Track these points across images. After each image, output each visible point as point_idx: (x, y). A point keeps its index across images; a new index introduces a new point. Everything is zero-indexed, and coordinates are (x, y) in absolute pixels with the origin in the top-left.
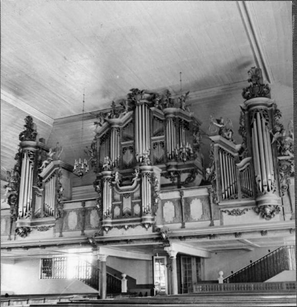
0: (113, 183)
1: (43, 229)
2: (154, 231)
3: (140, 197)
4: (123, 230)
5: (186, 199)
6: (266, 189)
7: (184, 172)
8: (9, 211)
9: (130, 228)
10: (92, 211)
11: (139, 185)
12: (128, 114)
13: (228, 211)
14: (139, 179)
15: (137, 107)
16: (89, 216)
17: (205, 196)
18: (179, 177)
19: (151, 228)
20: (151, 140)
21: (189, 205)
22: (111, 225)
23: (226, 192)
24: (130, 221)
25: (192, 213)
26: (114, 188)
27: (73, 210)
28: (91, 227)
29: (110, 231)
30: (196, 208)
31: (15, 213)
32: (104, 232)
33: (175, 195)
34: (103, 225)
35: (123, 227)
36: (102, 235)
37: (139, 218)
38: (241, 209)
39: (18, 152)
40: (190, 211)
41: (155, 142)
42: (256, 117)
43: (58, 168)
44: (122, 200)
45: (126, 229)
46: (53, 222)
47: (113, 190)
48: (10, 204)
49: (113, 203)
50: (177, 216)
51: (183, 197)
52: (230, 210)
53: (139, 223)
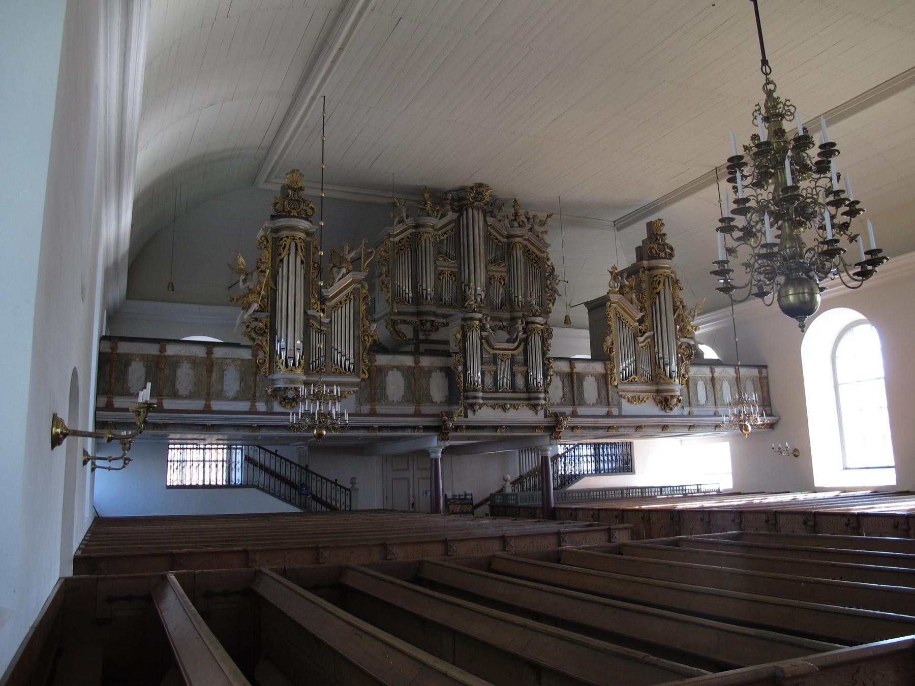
0: (484, 334)
2: (545, 417)
3: (526, 363)
5: (578, 374)
9: (512, 410)
10: (434, 374)
11: (523, 344)
12: (451, 216)
14: (525, 336)
15: (470, 211)
16: (428, 384)
19: (541, 413)
20: (487, 271)
22: (481, 401)
25: (586, 395)
27: (395, 367)
28: (433, 402)
32: (469, 412)
34: (470, 401)
36: (466, 416)
37: (524, 396)
40: (582, 393)
43: (359, 286)
44: (495, 363)
45: (504, 408)
46: (357, 385)
47: (481, 344)
48: (253, 339)
49: (483, 367)
50: (567, 397)
51: (575, 370)
52: (629, 395)
53: (526, 402)
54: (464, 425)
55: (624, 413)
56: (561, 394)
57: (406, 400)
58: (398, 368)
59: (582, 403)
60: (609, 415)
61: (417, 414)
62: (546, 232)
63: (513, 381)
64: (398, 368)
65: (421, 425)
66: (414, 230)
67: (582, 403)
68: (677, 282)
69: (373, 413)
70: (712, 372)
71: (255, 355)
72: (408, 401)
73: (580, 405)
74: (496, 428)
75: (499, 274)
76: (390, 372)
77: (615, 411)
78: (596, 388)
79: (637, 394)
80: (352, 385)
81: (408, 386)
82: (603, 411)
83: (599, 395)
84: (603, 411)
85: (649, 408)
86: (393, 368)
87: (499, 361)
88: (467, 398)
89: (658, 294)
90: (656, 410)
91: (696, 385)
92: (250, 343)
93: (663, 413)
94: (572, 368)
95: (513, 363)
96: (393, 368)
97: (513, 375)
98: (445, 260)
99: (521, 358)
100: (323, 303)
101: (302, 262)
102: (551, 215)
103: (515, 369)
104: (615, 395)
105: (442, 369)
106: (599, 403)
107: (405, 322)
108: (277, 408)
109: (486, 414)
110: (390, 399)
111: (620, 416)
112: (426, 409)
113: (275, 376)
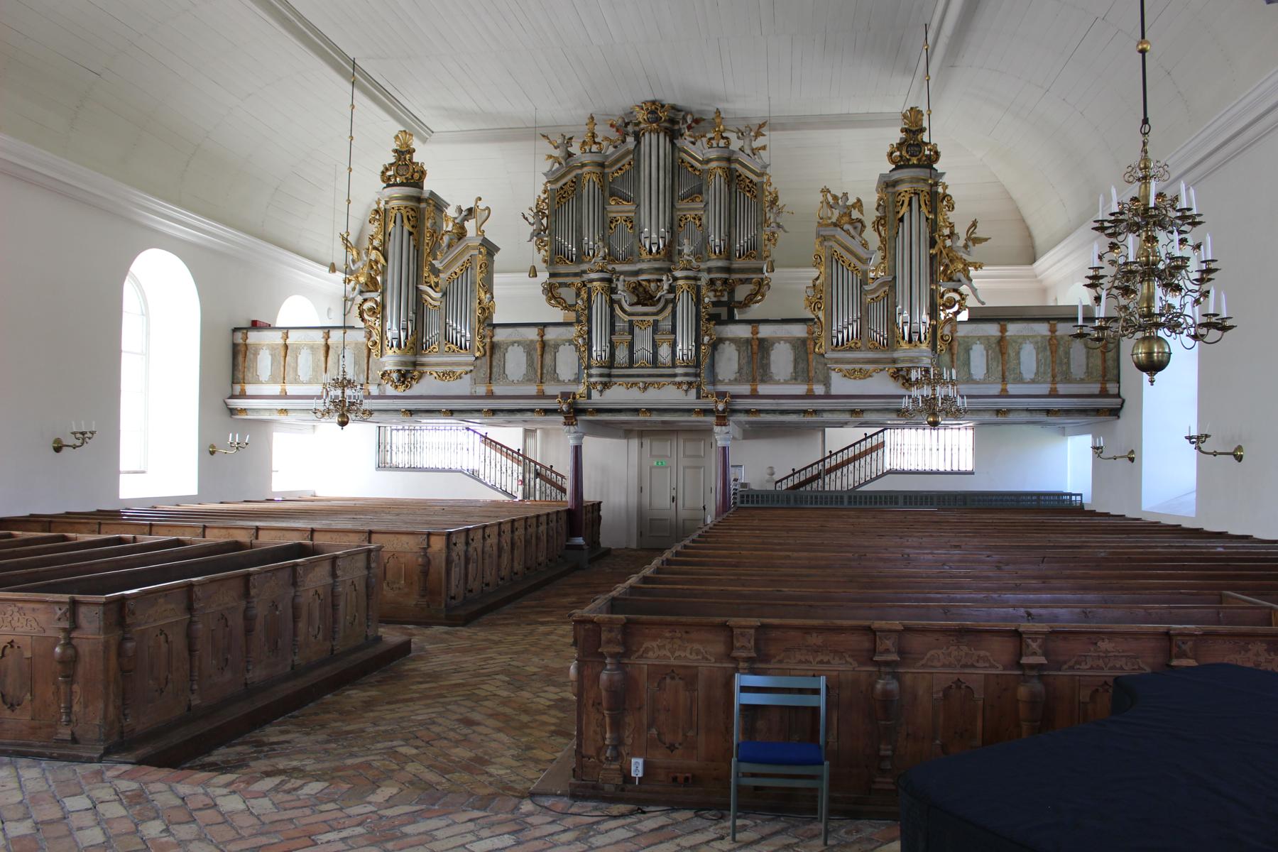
0: (614, 296)
1: (445, 375)
2: (698, 397)
4: (635, 389)
5: (762, 341)
6: (915, 337)
7: (743, 282)
8: (362, 333)
10: (561, 348)
13: (840, 370)
15: (647, 135)
17: (799, 339)
18: (732, 292)
19: (693, 392)
21: (769, 355)
23: (840, 336)
24: (650, 376)
25: (774, 369)
26: (616, 307)
29: (607, 392)
30: (782, 360)
31: (376, 337)
33: (743, 331)
35: (636, 384)
36: (589, 397)
38: (870, 367)
39: (375, 207)
41: (682, 213)
42: (910, 204)
44: (631, 332)
48: (363, 320)
50: (744, 371)
54: (590, 407)
55: (834, 392)
56: (736, 367)
57: (528, 380)
58: (519, 343)
59: (766, 377)
60: (810, 396)
61: (542, 396)
62: (764, 148)
63: (655, 354)
64: (519, 343)
65: (537, 407)
66: (579, 172)
67: (766, 377)
68: (945, 196)
69: (490, 396)
70: (1003, 330)
71: (369, 335)
72: (529, 380)
73: (763, 381)
74: (636, 411)
75: (693, 213)
76: (510, 348)
77: (819, 389)
78: (791, 357)
79: (857, 367)
80: (467, 364)
81: (530, 363)
82: (801, 389)
83: (795, 368)
84: (801, 389)
85: (881, 384)
86: (513, 343)
87: (637, 330)
88: (590, 376)
89: (901, 220)
90: (893, 388)
91: (968, 350)
92: (362, 325)
93: (902, 391)
94: (755, 332)
95: (655, 331)
96: (513, 343)
97: (655, 346)
98: (617, 203)
99: (666, 325)
100: (437, 276)
101: (410, 234)
102: (764, 124)
103: (657, 337)
104: (820, 367)
105: (570, 342)
106: (795, 379)
107: (561, 285)
108: (390, 390)
109: (618, 395)
110: (510, 378)
111: (827, 396)
112: (551, 389)
113: (384, 359)
